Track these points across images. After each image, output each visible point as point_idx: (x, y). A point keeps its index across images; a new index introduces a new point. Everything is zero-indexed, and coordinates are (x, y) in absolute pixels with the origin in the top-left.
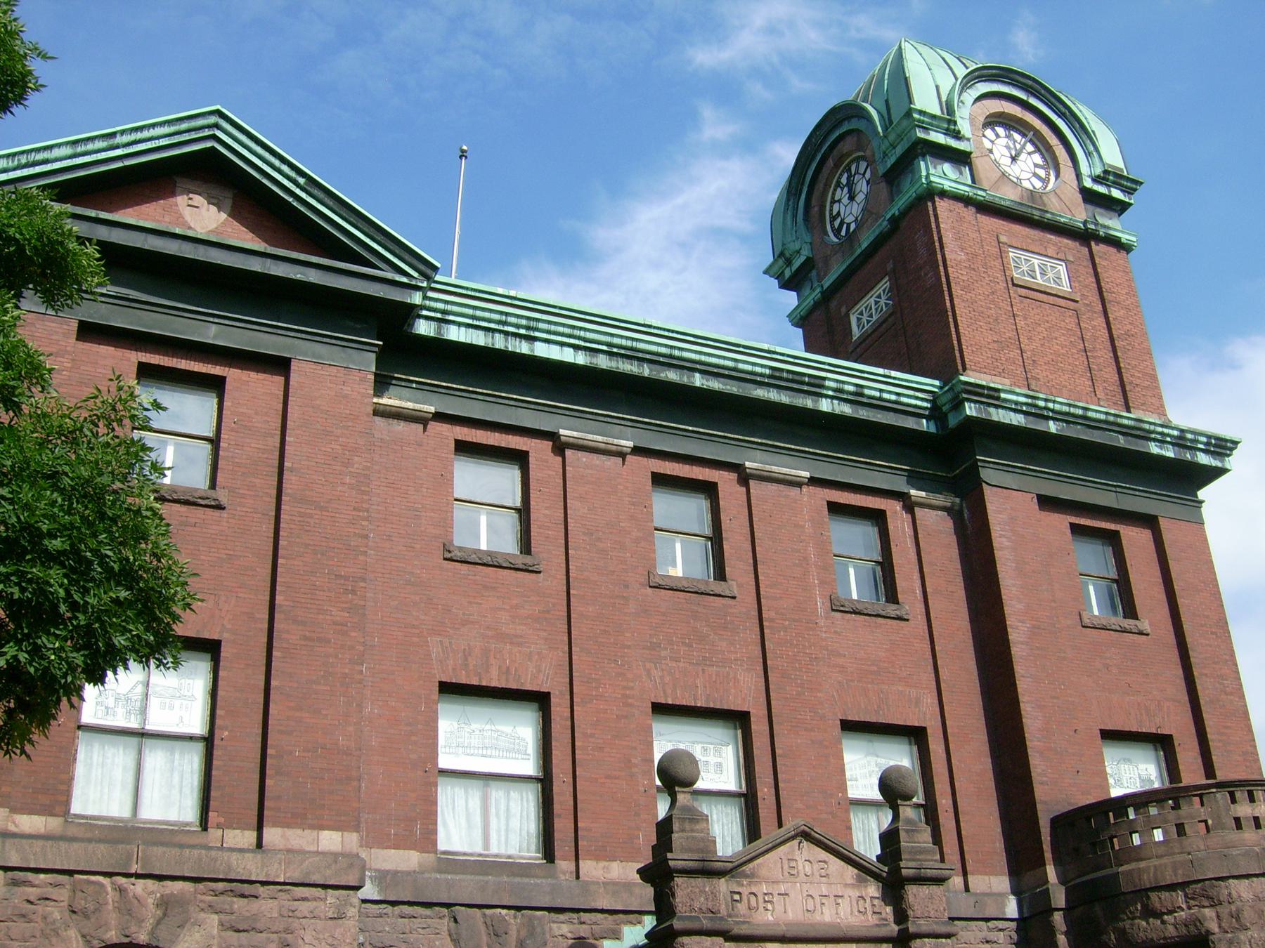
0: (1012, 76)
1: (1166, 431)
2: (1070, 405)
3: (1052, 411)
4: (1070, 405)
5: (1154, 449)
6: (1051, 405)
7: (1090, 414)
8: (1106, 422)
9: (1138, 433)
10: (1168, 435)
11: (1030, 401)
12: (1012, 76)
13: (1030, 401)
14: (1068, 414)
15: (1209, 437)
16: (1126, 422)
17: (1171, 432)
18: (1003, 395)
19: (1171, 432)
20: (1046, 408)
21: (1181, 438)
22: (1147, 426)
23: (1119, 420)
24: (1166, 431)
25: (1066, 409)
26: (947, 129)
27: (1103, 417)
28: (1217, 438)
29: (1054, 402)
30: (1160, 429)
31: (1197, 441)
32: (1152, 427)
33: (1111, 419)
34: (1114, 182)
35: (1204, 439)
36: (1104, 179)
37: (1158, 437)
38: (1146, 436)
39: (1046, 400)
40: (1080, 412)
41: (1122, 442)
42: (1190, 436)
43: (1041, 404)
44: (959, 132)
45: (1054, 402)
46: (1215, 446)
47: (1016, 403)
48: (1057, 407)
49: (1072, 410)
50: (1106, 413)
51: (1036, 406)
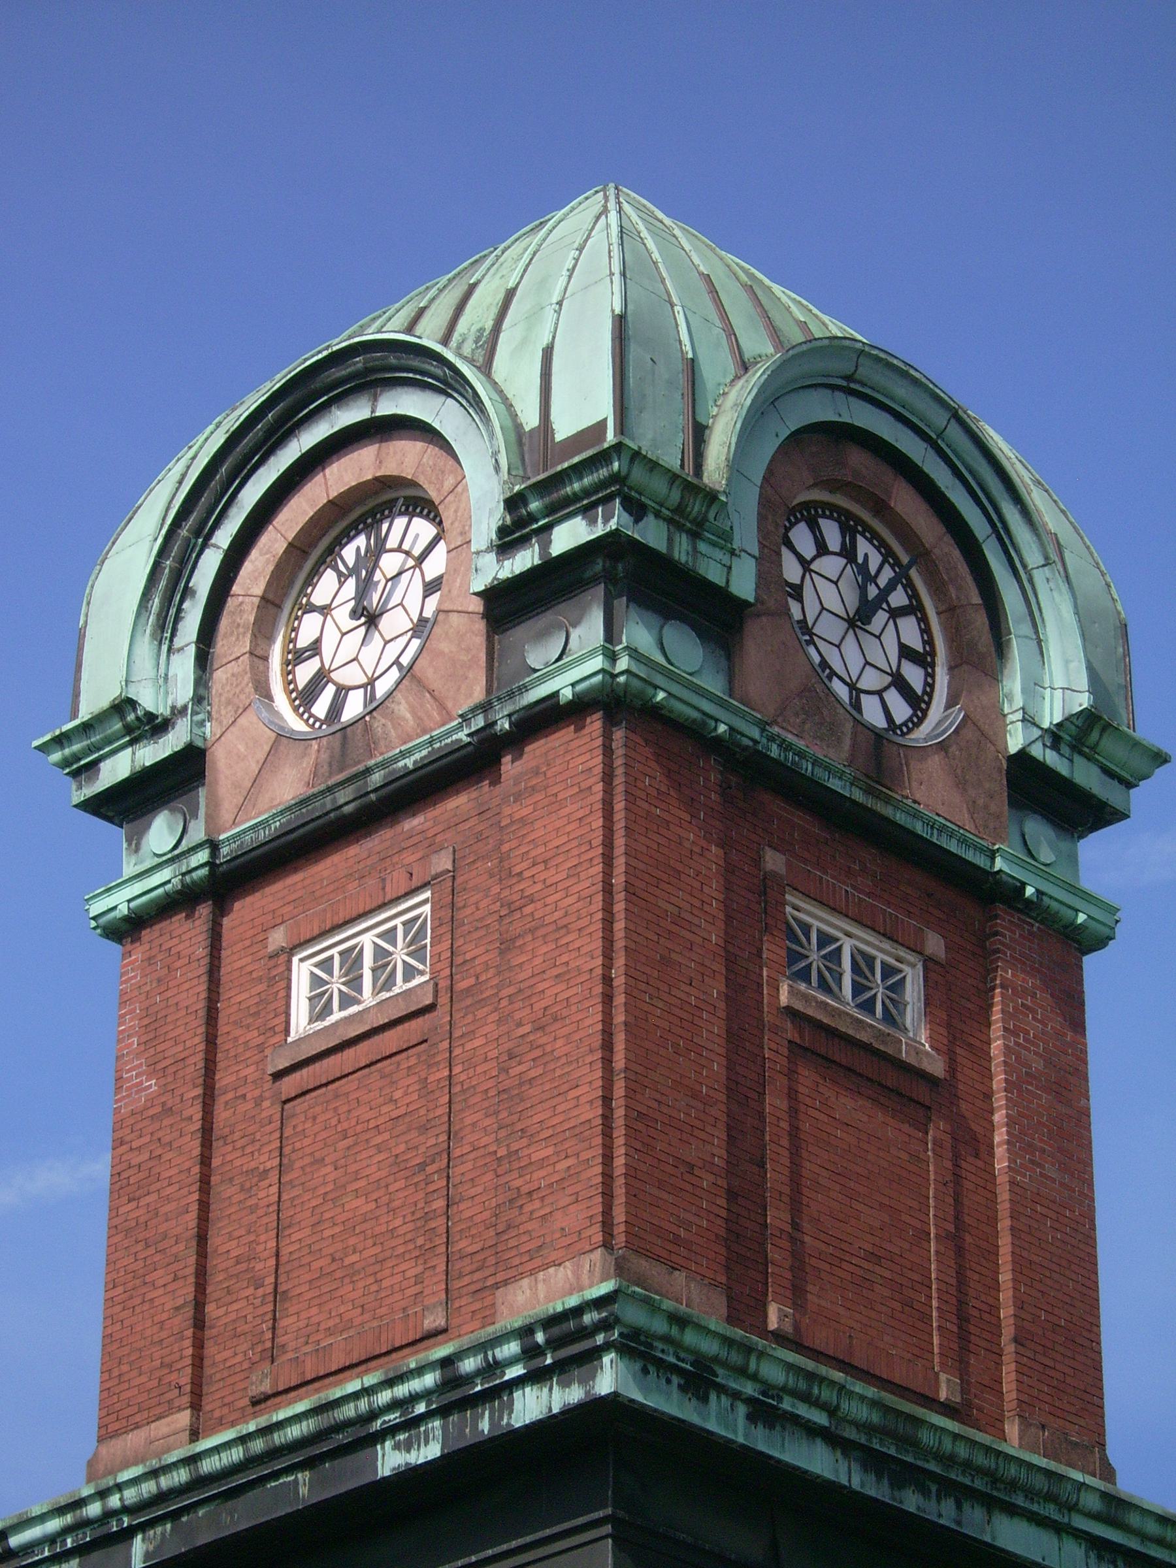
0: (317, 384)
1: (401, 1391)
2: (154, 1474)
3: (126, 1510)
4: (154, 1474)
5: (390, 1459)
6: (114, 1501)
7: (208, 1466)
8: (249, 1462)
9: (341, 1438)
10: (414, 1398)
11: (69, 1519)
12: (317, 384)
13: (69, 1519)
14: (161, 1497)
15: (526, 1332)
16: (294, 1432)
17: (416, 1385)
18: (15, 1541)
19: (416, 1385)
20: (108, 1514)
21: (452, 1381)
22: (349, 1411)
23: (278, 1438)
24: (401, 1391)
25: (148, 1488)
26: (128, 729)
27: (236, 1454)
28: (550, 1322)
29: (119, 1487)
30: (384, 1397)
31: (494, 1367)
32: (363, 1405)
33: (258, 1446)
34: (551, 510)
35: (512, 1348)
36: (520, 523)
37: (393, 1417)
38: (364, 1437)
39: (102, 1494)
40: (182, 1476)
41: (304, 1487)
42: (469, 1365)
43: (94, 1509)
44: (150, 716)
45: (119, 1487)
46: (554, 1344)
47: (51, 1539)
48: (131, 1495)
49: (165, 1482)
50: (243, 1440)
51: (86, 1523)
